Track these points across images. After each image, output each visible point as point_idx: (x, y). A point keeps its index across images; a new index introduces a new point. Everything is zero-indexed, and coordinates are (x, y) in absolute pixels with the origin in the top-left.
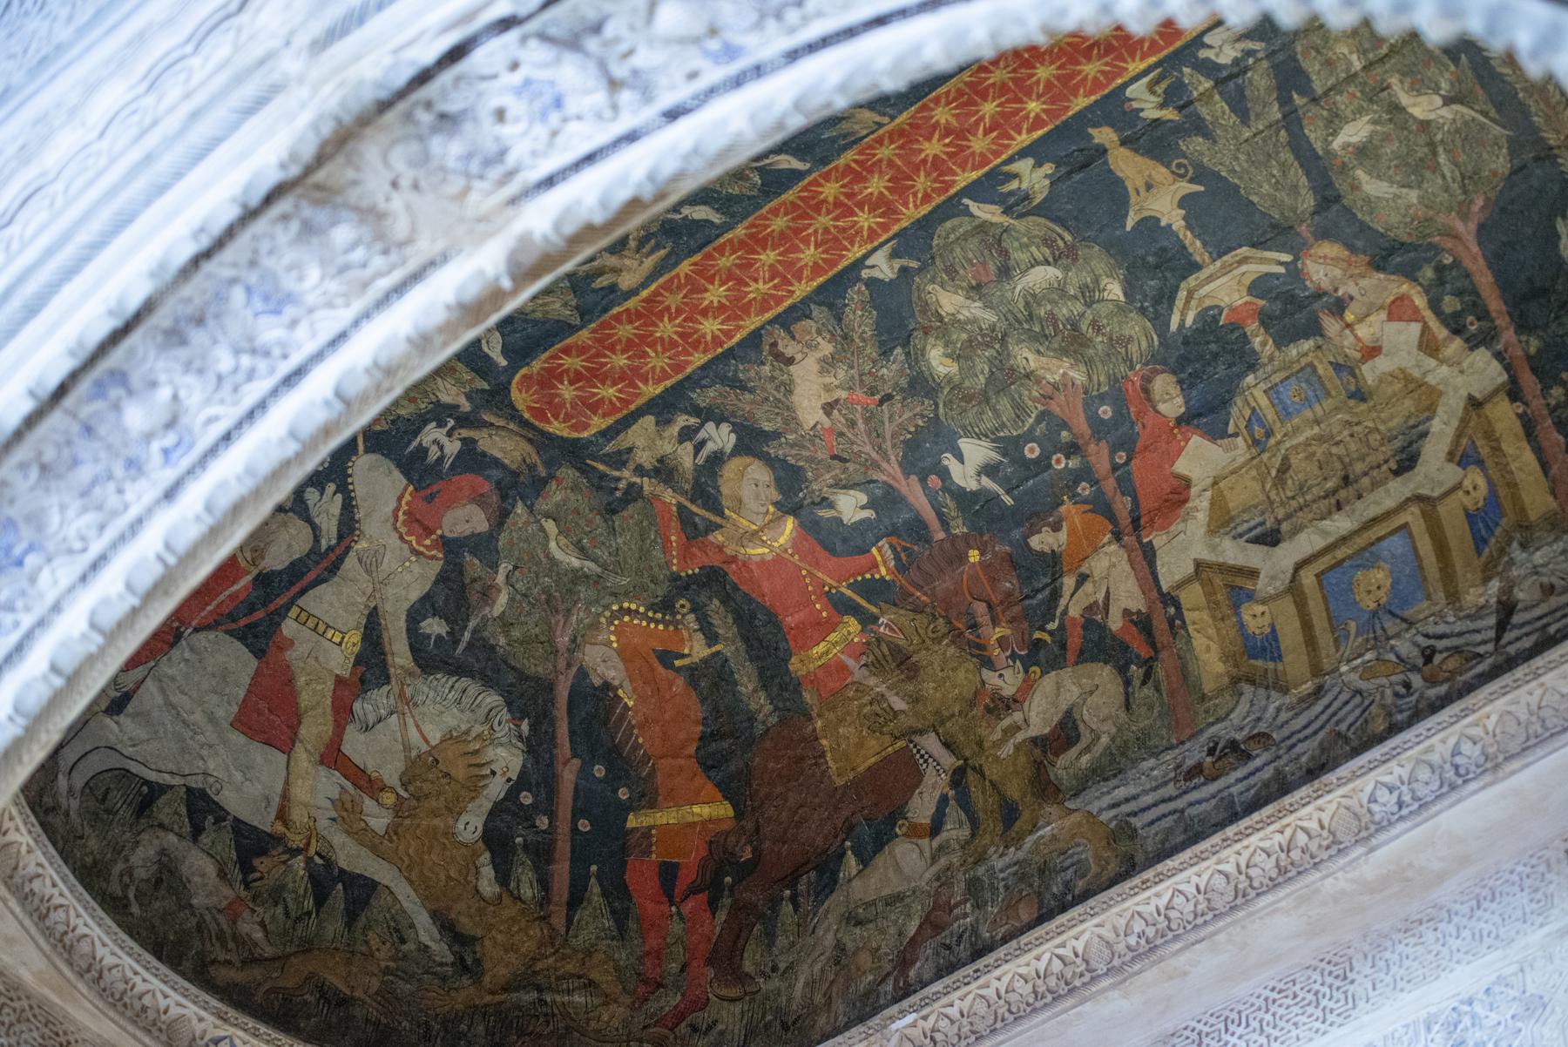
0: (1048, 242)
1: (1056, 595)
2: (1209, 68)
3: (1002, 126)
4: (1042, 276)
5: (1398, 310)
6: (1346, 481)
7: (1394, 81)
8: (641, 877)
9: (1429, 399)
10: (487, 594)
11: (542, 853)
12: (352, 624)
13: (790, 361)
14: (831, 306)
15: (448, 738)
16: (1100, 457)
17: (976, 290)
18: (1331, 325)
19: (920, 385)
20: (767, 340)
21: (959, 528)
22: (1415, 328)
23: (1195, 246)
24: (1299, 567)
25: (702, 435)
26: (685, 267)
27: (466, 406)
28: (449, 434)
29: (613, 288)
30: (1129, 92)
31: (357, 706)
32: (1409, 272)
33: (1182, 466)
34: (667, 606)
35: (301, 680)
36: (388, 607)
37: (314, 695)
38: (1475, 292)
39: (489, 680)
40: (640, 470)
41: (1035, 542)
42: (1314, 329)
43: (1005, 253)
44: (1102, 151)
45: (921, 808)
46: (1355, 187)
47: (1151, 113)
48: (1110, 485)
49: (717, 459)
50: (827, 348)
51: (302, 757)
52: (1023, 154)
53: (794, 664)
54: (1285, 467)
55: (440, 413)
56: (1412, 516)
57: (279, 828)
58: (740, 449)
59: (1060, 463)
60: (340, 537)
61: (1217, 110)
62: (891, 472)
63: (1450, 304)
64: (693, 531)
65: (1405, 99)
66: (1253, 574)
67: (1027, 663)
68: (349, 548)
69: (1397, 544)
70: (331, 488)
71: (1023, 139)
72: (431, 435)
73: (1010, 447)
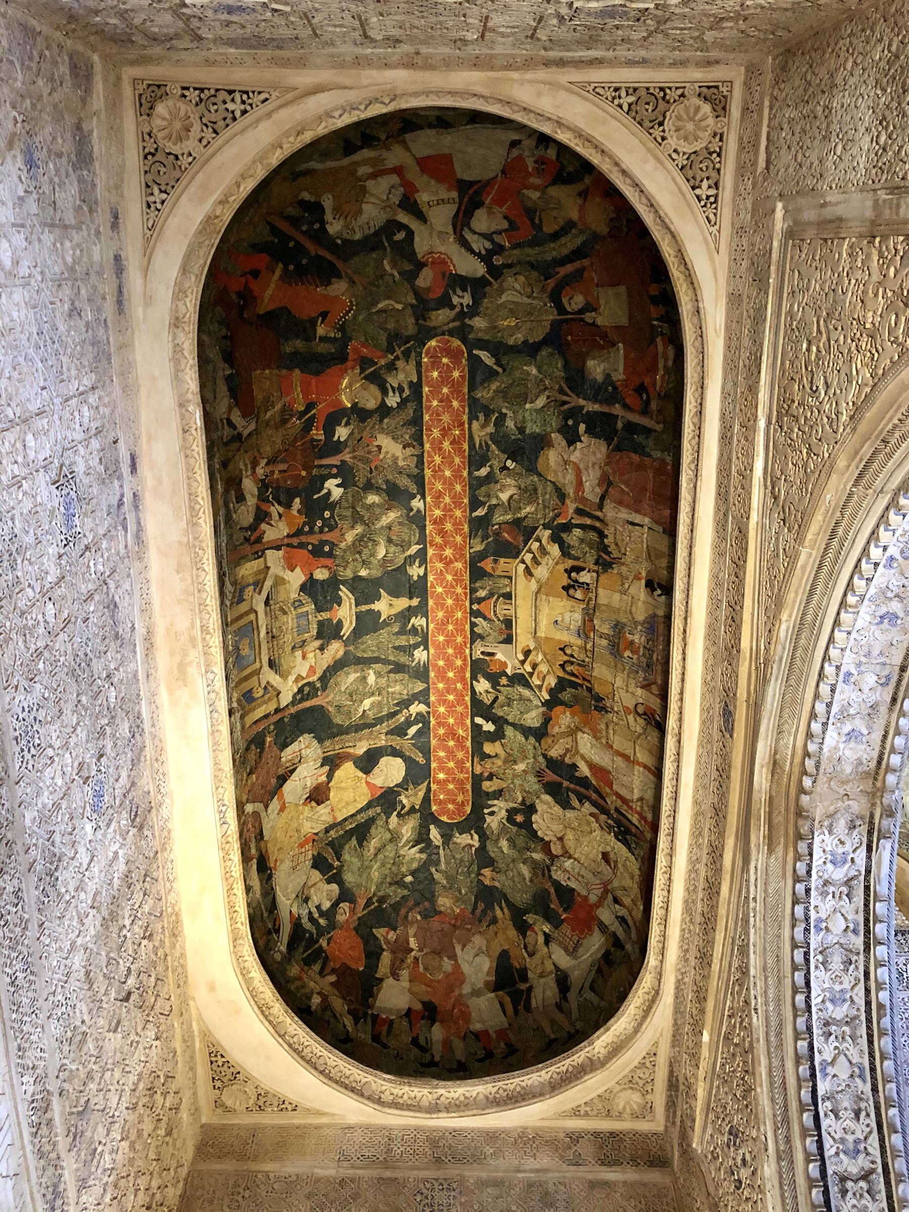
0: (391, 561)
1: (280, 504)
2: (416, 646)
3: (441, 575)
4: (381, 552)
5: (312, 670)
6: (273, 637)
7: (379, 698)
8: (261, 261)
9: (284, 676)
10: (394, 265)
11: (295, 222)
12: (430, 213)
13: (404, 448)
14: (415, 476)
15: (360, 212)
16: (314, 539)
17: (389, 528)
18: (317, 643)
19: (369, 486)
20: (417, 446)
21: (314, 472)
22: (304, 675)
23: (364, 608)
24: (256, 612)
25: (397, 394)
26: (466, 446)
27: (467, 321)
28: (462, 304)
29: (477, 419)
30: (424, 619)
31: (402, 189)
32: (320, 679)
33: (298, 570)
34: (342, 329)
35: (433, 182)
36: (422, 227)
37: (419, 179)
38: (307, 699)
39: (366, 239)
40: (397, 358)
41: (297, 500)
42: (319, 636)
43: (396, 545)
44: (411, 598)
45: (236, 417)
46: (355, 672)
47: (413, 620)
48: (304, 539)
49: (385, 392)
50: (401, 463)
51: (409, 161)
52: (426, 574)
53: (297, 372)
54: (285, 613)
55: (474, 310)
56: (257, 665)
57: (401, 138)
58: (383, 403)
59: (319, 523)
60: (462, 236)
61: (402, 641)
62: (347, 456)
63: (307, 689)
64: (365, 363)
65: (372, 699)
66: (260, 593)
67: (263, 481)
68: (455, 233)
69: (252, 658)
70: (483, 252)
71: (431, 578)
72: (467, 300)
73: (332, 507)
